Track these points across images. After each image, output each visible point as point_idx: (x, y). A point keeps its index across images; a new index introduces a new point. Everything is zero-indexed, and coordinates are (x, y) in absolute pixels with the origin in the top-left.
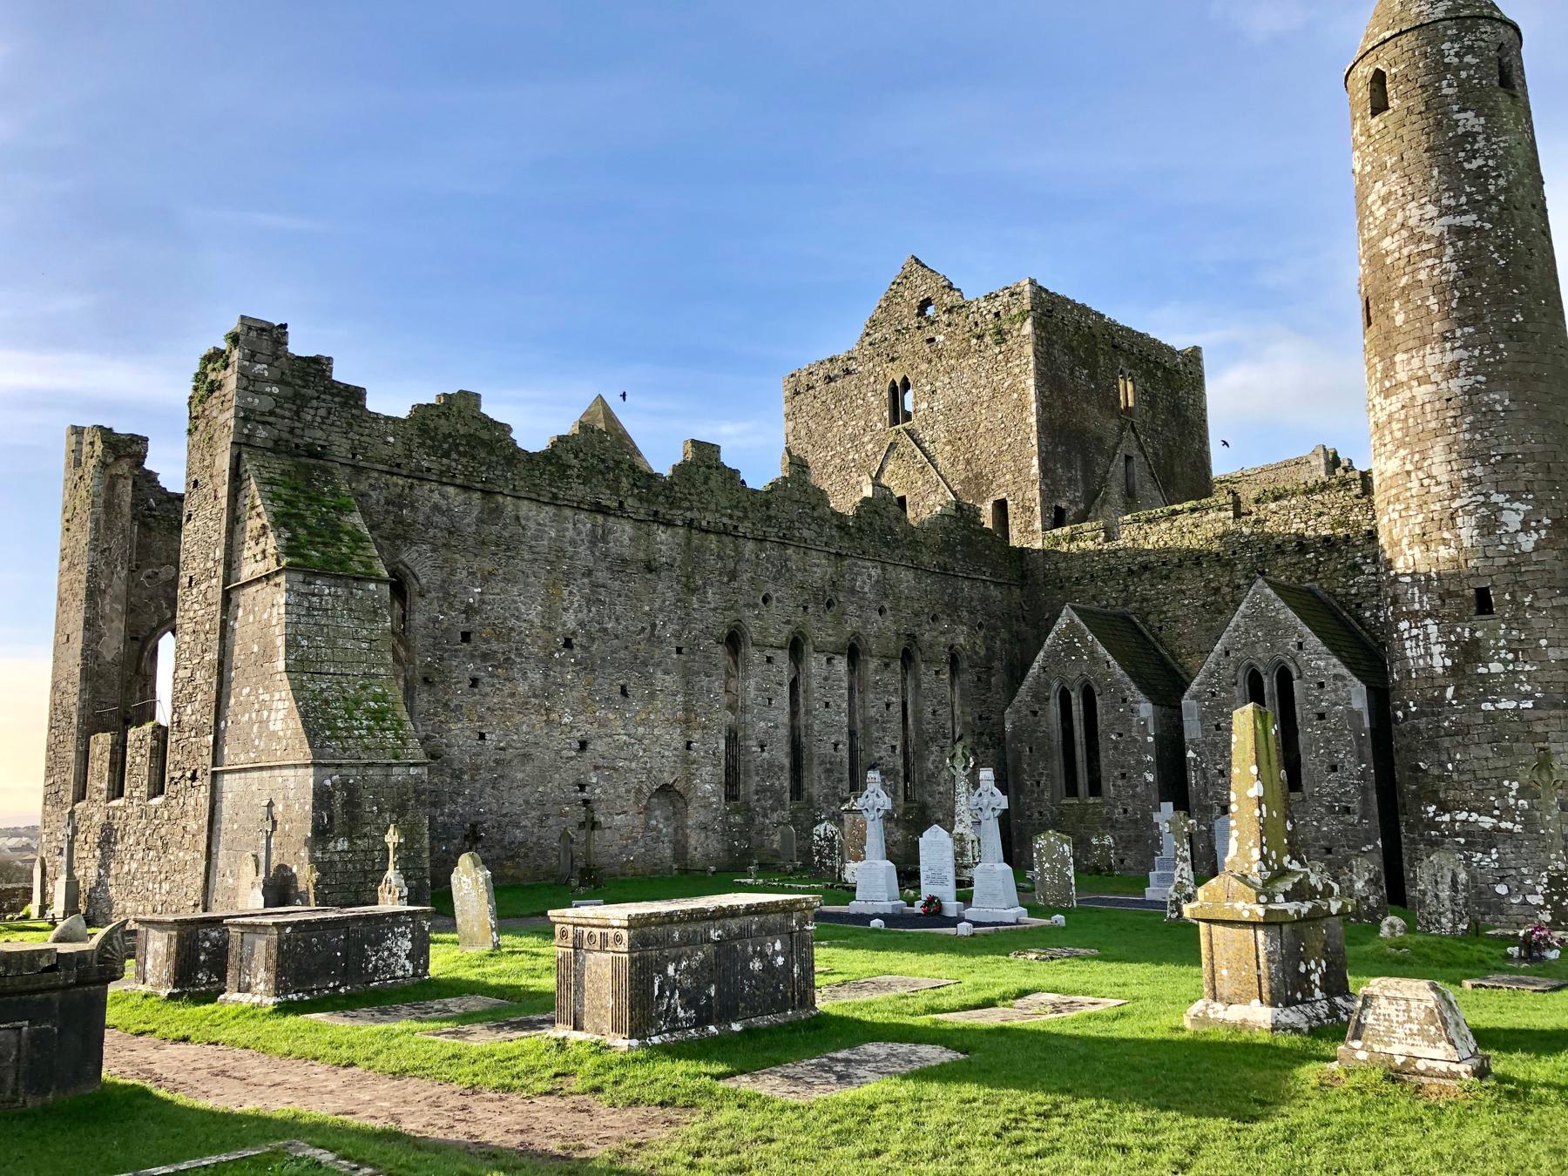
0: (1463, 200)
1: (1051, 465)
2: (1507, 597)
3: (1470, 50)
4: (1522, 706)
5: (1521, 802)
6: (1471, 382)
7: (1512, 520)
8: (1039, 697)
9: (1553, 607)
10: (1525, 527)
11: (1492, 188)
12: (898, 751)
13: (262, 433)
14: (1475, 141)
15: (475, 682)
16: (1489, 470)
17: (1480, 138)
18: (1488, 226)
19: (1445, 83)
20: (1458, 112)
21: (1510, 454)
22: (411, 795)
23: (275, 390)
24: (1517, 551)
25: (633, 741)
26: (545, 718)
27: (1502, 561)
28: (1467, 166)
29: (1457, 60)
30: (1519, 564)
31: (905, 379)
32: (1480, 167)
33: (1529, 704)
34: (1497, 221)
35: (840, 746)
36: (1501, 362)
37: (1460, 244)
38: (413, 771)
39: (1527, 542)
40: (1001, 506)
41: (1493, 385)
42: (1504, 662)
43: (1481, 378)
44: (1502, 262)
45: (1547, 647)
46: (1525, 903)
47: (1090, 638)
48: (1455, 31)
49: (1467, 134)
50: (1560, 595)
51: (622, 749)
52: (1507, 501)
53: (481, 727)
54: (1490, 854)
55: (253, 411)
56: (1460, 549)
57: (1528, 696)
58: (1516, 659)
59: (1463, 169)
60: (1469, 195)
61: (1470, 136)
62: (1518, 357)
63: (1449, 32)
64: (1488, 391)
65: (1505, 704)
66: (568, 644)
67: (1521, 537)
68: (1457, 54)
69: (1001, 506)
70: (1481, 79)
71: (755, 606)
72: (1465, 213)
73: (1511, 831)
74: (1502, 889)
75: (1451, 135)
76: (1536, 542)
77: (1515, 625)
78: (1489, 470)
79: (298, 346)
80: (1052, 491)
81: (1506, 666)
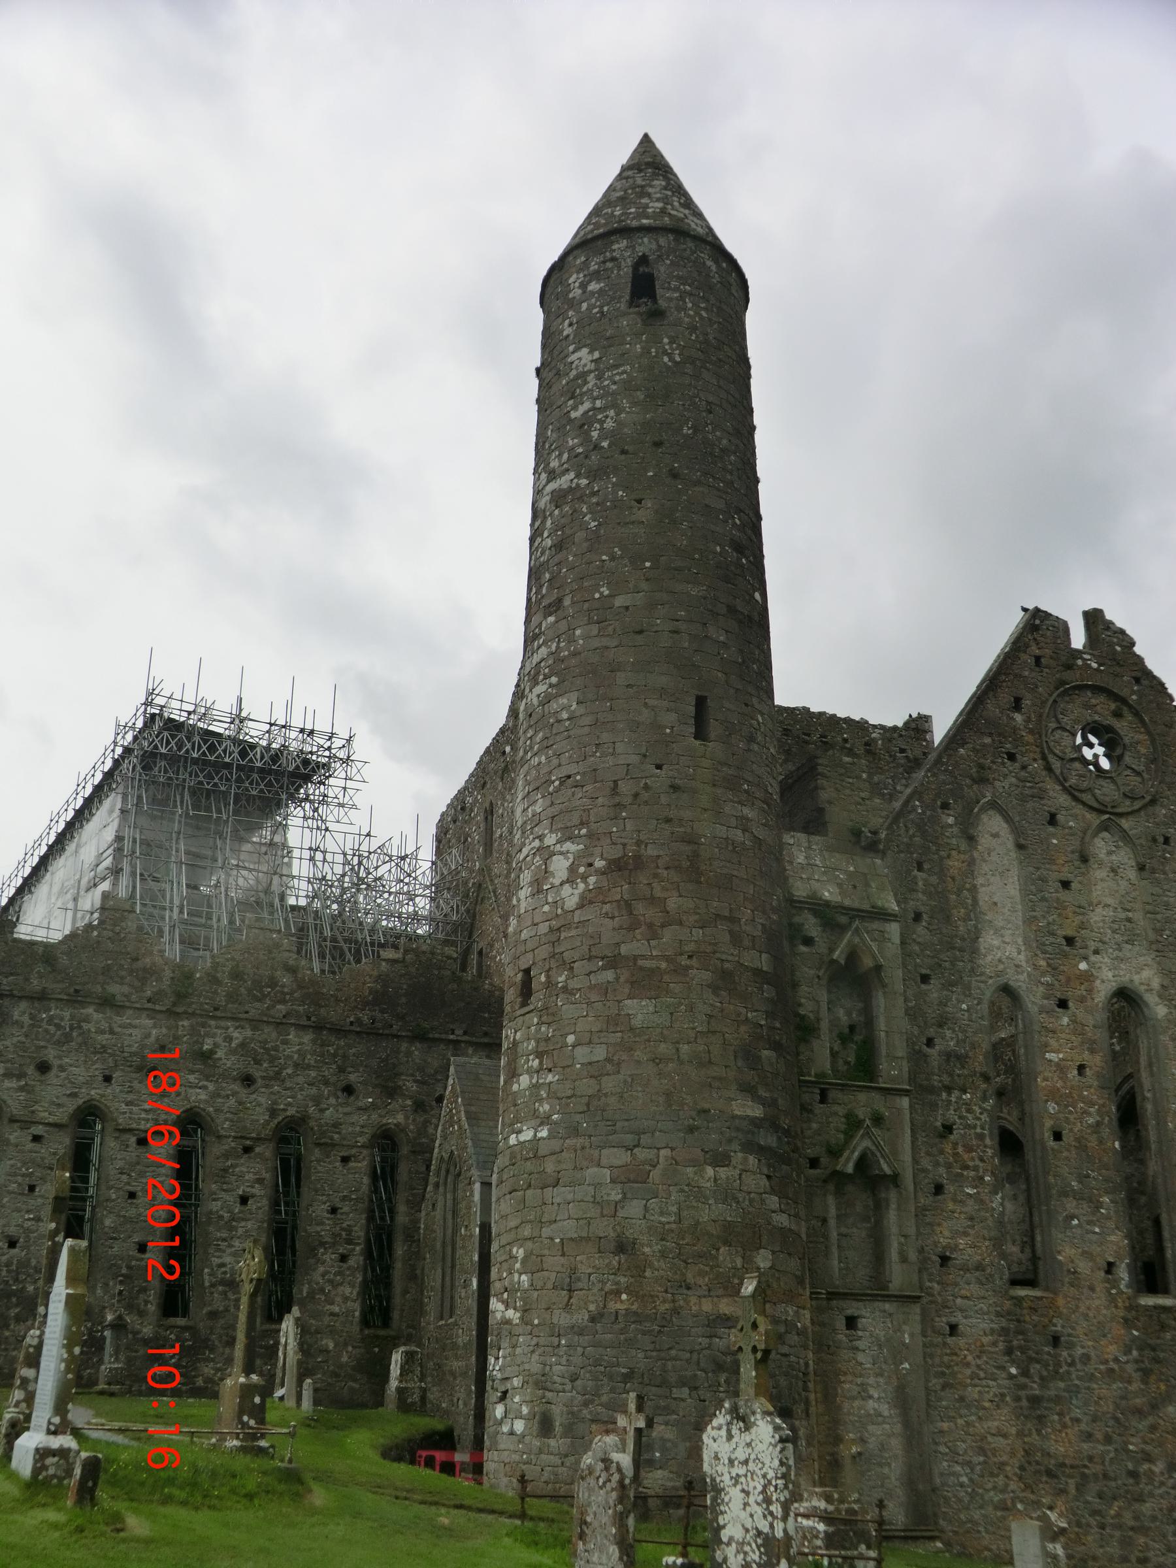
0: (565, 456)
2: (543, 979)
3: (596, 276)
4: (539, 1135)
5: (524, 1277)
9: (591, 987)
10: (572, 877)
11: (595, 434)
14: (586, 382)
18: (584, 482)
19: (567, 322)
20: (573, 352)
21: (569, 777)
27: (543, 928)
28: (573, 415)
29: (580, 291)
30: (559, 929)
32: (586, 412)
33: (544, 1133)
36: (575, 654)
37: (557, 512)
39: (571, 896)
42: (530, 1071)
43: (554, 680)
44: (593, 524)
45: (574, 1046)
46: (512, 1433)
48: (583, 259)
49: (577, 377)
50: (604, 968)
52: (558, 842)
57: (545, 1120)
59: (571, 421)
61: (583, 375)
62: (596, 643)
63: (578, 262)
65: (527, 1135)
67: (567, 890)
68: (583, 286)
70: (601, 307)
71: (21, 1076)
72: (567, 470)
75: (564, 382)
76: (582, 897)
77: (544, 1018)
81: (531, 1078)
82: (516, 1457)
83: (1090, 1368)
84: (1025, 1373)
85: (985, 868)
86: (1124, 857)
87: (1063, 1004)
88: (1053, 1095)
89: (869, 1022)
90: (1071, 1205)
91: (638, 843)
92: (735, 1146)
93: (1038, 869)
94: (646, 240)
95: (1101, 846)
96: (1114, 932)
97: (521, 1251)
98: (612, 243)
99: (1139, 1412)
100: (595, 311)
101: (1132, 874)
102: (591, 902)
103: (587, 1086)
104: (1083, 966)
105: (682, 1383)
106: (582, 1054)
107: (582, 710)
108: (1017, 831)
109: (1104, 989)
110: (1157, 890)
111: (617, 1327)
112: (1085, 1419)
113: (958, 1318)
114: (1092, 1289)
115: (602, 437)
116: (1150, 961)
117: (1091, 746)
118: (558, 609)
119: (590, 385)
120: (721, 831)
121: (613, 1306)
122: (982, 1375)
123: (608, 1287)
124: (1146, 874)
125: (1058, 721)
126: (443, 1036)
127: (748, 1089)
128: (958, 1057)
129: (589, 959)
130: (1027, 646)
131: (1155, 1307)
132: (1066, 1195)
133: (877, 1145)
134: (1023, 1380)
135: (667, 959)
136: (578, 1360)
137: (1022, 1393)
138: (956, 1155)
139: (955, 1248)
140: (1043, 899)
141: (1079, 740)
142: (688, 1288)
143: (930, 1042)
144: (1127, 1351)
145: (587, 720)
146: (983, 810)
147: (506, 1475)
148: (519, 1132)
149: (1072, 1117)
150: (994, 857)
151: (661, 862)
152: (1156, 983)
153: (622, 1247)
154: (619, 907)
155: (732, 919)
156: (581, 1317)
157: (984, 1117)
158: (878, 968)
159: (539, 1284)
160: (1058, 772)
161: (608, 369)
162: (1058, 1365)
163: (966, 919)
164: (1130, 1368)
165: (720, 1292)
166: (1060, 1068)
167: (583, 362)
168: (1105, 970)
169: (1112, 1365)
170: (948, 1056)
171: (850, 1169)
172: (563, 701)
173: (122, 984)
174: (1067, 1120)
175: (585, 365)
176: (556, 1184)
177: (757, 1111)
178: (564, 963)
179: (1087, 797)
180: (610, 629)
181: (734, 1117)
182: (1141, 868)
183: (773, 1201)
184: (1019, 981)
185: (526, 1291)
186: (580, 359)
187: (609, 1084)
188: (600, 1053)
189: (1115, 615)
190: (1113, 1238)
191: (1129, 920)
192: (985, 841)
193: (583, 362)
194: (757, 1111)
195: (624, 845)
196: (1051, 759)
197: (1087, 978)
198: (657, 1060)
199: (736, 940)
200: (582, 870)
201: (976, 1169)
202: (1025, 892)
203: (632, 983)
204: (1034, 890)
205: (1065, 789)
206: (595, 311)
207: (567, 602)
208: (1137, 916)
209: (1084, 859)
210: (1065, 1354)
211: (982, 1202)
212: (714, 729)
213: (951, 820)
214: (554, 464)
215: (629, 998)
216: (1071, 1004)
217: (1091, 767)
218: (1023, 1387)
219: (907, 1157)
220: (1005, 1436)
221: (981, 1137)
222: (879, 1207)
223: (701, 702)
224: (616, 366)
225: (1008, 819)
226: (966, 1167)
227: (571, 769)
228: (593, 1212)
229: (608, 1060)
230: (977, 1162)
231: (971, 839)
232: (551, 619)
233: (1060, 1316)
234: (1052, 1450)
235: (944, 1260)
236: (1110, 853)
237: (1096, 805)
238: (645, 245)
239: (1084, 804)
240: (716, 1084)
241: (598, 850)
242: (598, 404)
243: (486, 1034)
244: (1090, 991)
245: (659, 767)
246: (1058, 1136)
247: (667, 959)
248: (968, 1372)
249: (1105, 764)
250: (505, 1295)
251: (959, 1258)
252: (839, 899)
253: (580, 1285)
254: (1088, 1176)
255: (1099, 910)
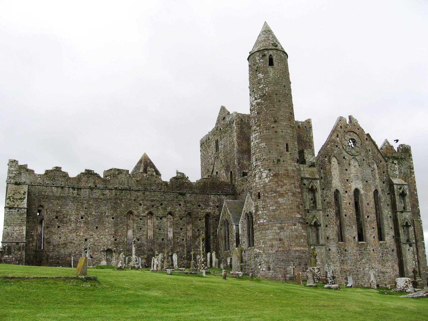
0: (258, 96)
1: (241, 161)
2: (263, 195)
4: (264, 222)
5: (263, 245)
6: (258, 141)
7: (264, 175)
8: (221, 225)
11: (264, 92)
12: (185, 240)
13: (12, 181)
14: (262, 81)
15: (59, 227)
16: (261, 163)
17: (262, 80)
18: (263, 102)
20: (258, 74)
22: (22, 248)
23: (15, 172)
24: (265, 183)
25: (99, 239)
26: (76, 234)
27: (262, 186)
28: (260, 87)
29: (259, 61)
31: (217, 139)
32: (262, 87)
34: (265, 100)
35: (164, 240)
36: (263, 136)
37: (258, 107)
38: (22, 244)
39: (267, 180)
40: (231, 172)
41: (262, 142)
42: (261, 211)
43: (260, 140)
44: (265, 110)
45: (269, 207)
46: (263, 270)
47: (227, 209)
49: (259, 79)
50: (274, 193)
51: (97, 241)
53: (60, 236)
54: (258, 259)
55: (11, 177)
56: (256, 183)
57: (265, 219)
58: (263, 210)
60: (260, 94)
61: (261, 79)
62: (268, 134)
64: (261, 143)
65: (262, 221)
66: (82, 218)
68: (259, 60)
69: (231, 172)
70: (263, 65)
73: (261, 253)
74: (260, 267)
77: (263, 202)
78: (261, 163)
79: (20, 163)
80: (242, 168)
82: (264, 274)
83: (351, 255)
84: (341, 256)
85: (333, 168)
86: (356, 164)
87: (346, 192)
88: (345, 208)
89: (315, 198)
90: (348, 227)
91: (278, 171)
92: (297, 222)
93: (342, 167)
94: (271, 51)
95: (352, 162)
96: (355, 178)
97: (262, 241)
98: (264, 52)
99: (359, 261)
100: (262, 66)
101: (358, 167)
102: (271, 182)
103: (272, 213)
104: (350, 185)
105: (291, 261)
106: (271, 208)
107: (266, 146)
108: (338, 160)
109: (353, 189)
110: (362, 170)
111: (280, 253)
112: (350, 263)
113: (330, 248)
114: (351, 241)
115: (266, 92)
116: (361, 183)
117: (350, 143)
118: (260, 126)
119: (263, 81)
120: (292, 168)
121: (280, 249)
122: (334, 257)
123: (278, 246)
124: (360, 166)
125: (345, 138)
126: (217, 193)
127: (298, 212)
128: (329, 203)
129: (271, 191)
130: (339, 124)
131: (361, 244)
132: (347, 226)
133: (318, 220)
134: (341, 257)
135: (285, 191)
136: (274, 258)
137: (340, 259)
138: (329, 220)
139: (330, 236)
140: (343, 173)
141: (348, 142)
142: (291, 246)
143: (324, 201)
144: (357, 251)
145: (268, 148)
146: (332, 157)
147: (262, 277)
148: (260, 221)
149: (348, 212)
150: (334, 166)
151: (282, 174)
152: (362, 187)
153: (280, 240)
154: (276, 182)
155: (294, 184)
156: (274, 251)
157: (334, 213)
158: (316, 189)
159: (266, 246)
160: (345, 148)
161: (266, 79)
162: (346, 254)
163: (330, 177)
164: (357, 254)
165: (296, 246)
166: (346, 204)
167: (261, 76)
168: (353, 185)
169: (355, 254)
170: (328, 203)
171: (313, 224)
172: (262, 144)
173: (154, 187)
174: (347, 213)
175: (261, 77)
176: (268, 230)
177: (300, 216)
178: (267, 192)
179: (350, 153)
180: (271, 131)
181: (296, 217)
182: (359, 166)
183: (303, 231)
184: (339, 189)
185: (264, 247)
186: (260, 76)
187: (276, 213)
188: (274, 208)
189: (355, 117)
190: (355, 233)
191: (357, 176)
192: (333, 163)
193: (261, 76)
194: (300, 216)
195: (276, 171)
196: (344, 146)
197: (350, 187)
198: (284, 209)
199: (295, 187)
200: (269, 176)
201: (332, 222)
202: (340, 172)
203: (279, 196)
204: (341, 172)
205: (346, 152)
206: (262, 66)
207: (262, 125)
208: (359, 175)
209: (350, 165)
210: (347, 252)
211: (334, 228)
212: (290, 149)
213: (327, 159)
214: (256, 96)
215: (279, 198)
216: (348, 192)
217: (350, 147)
218: (341, 258)
219: (322, 221)
220: (338, 266)
221: (333, 217)
222: (318, 230)
223: (287, 144)
224: (268, 78)
225: (336, 158)
226: (331, 222)
227: (265, 157)
228: (275, 234)
229: (276, 209)
230: (333, 221)
231: (330, 163)
232: (258, 128)
233: (346, 246)
234: (345, 268)
235: (328, 238)
236: (354, 163)
237: (352, 155)
238: (271, 52)
239: (350, 154)
240: (294, 212)
241: (271, 172)
242: (264, 86)
243: (225, 192)
244: (351, 189)
245: (281, 157)
246: (346, 216)
247: (285, 191)
248: (332, 257)
249: (353, 146)
250: (259, 248)
251: (331, 238)
252: (309, 177)
253: (274, 246)
254: (351, 222)
255: (352, 174)
